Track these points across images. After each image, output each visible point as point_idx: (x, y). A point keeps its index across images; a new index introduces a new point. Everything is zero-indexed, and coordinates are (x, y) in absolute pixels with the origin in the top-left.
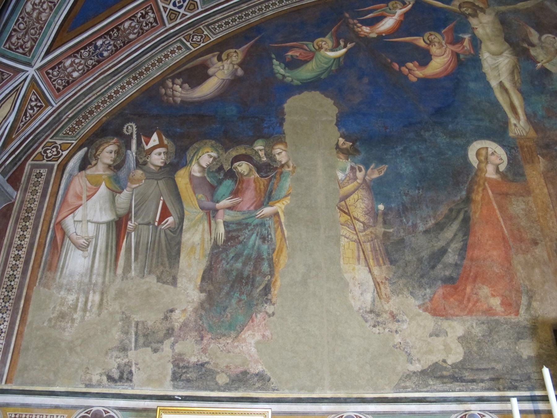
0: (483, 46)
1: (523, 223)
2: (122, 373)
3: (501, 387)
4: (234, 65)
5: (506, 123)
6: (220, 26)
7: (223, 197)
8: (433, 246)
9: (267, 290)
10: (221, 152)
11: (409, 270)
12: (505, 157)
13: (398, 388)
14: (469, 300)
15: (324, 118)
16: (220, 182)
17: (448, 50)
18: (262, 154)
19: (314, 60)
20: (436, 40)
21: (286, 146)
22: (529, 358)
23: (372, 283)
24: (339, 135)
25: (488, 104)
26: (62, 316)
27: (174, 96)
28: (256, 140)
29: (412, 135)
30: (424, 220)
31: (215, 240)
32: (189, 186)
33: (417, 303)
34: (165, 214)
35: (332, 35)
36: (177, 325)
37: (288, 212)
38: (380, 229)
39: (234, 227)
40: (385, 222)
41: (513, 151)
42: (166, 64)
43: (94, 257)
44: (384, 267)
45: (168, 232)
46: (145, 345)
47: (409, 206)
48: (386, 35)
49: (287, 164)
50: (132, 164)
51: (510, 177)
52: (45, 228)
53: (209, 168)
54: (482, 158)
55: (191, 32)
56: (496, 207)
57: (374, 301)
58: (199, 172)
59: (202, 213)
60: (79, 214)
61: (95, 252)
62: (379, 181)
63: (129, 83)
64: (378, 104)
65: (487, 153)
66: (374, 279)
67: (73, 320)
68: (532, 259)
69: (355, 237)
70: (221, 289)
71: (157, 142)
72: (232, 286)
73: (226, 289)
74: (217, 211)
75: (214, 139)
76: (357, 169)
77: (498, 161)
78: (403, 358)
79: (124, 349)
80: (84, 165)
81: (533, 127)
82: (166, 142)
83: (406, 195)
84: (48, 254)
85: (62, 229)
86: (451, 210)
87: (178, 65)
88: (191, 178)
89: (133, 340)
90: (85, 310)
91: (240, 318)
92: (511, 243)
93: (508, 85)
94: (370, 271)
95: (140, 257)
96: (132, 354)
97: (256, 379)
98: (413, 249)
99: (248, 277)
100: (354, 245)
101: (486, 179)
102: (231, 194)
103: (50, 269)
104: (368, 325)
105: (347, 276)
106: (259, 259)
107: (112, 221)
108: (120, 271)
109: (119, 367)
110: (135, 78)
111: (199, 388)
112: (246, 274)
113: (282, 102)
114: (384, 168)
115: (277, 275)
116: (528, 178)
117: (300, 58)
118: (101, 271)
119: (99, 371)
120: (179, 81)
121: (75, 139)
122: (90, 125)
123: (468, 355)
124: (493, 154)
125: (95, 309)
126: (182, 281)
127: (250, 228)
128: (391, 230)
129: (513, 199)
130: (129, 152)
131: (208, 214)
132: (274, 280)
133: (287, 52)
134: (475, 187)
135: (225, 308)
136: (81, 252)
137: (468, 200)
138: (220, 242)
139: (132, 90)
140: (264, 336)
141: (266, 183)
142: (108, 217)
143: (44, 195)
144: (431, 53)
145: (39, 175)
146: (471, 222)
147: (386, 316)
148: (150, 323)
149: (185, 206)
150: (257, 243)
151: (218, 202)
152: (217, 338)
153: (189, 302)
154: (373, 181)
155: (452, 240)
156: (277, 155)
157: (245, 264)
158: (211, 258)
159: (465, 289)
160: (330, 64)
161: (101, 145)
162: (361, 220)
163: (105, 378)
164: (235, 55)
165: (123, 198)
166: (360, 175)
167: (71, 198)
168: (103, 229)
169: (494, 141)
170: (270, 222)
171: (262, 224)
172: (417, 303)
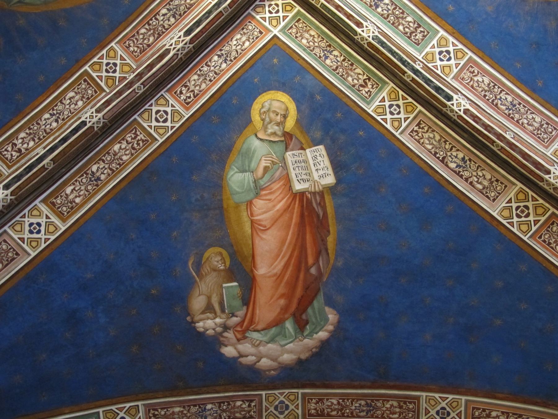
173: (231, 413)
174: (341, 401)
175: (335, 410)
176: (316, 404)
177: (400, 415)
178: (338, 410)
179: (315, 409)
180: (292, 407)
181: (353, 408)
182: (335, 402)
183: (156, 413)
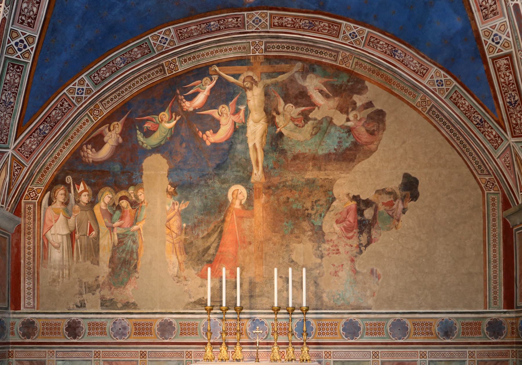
0: (250, 117)
1: (247, 233)
2: (81, 304)
4: (117, 134)
5: (251, 173)
6: (108, 102)
7: (116, 221)
8: (205, 245)
9: (136, 267)
10: (114, 194)
11: (193, 257)
12: (246, 196)
14: (216, 271)
15: (162, 173)
16: (114, 212)
17: (230, 119)
18: (132, 195)
19: (158, 130)
20: (225, 112)
21: (144, 190)
23: (177, 263)
24: (168, 183)
25: (244, 160)
26: (54, 281)
27: (88, 157)
28: (129, 187)
29: (203, 182)
30: (203, 232)
32: (100, 214)
33: (196, 272)
34: (91, 230)
35: (168, 111)
36: (101, 283)
37: (144, 228)
38: (183, 237)
39: (121, 236)
40: (185, 233)
41: (251, 191)
42: (81, 133)
43: (63, 252)
44: (183, 256)
45: (93, 239)
46: (89, 292)
47: (196, 224)
48: (198, 109)
49: (144, 201)
50: (73, 202)
51: (246, 206)
52: (39, 238)
53: (109, 204)
54: (235, 196)
55: (92, 107)
56: (236, 225)
57: (178, 271)
58: (105, 207)
59: (107, 229)
60: (53, 230)
61: (63, 250)
62: (186, 211)
63: (64, 148)
64: (188, 162)
66: (179, 261)
67: (59, 282)
68: (247, 252)
69: (172, 241)
70: (117, 267)
71: (83, 189)
72: (122, 265)
73: (119, 266)
74: (113, 228)
75: (110, 186)
77: (242, 198)
79: (81, 294)
80: (50, 202)
81: (265, 175)
82: (87, 188)
83: (196, 218)
84: (42, 252)
85: (46, 238)
86: (215, 226)
87: (88, 134)
88: (101, 209)
89: (84, 290)
90: (63, 277)
91: (126, 279)
92: (239, 243)
93: (258, 146)
94: (177, 258)
95: (83, 252)
96: (84, 296)
97: (132, 305)
98: (196, 247)
99: (128, 261)
100: (171, 245)
101: (234, 209)
102: (119, 219)
103: (45, 259)
104: (175, 282)
105: (168, 260)
106: (132, 252)
107: (68, 234)
108: (75, 259)
109: (80, 302)
110: (67, 144)
111: (111, 309)
112: (127, 259)
113: (142, 162)
114: (188, 203)
115: (139, 259)
116: (255, 207)
117: (151, 129)
118: (67, 259)
119: (72, 303)
120: (90, 146)
121: (42, 186)
122: (48, 177)
124: (240, 193)
125: (67, 277)
126: (101, 263)
127: (128, 237)
128: (188, 237)
129: (245, 219)
130: (70, 194)
131: (110, 230)
132: (138, 262)
133: (144, 125)
134: (228, 213)
135: (119, 275)
136: (56, 250)
137: (223, 221)
138: (116, 244)
139: (66, 153)
140: (135, 287)
141: (135, 212)
142: (66, 232)
143: (34, 220)
144: (221, 123)
145: (29, 208)
146: (223, 233)
147: (182, 278)
148: (90, 283)
149: (99, 226)
151: (114, 223)
152: (116, 288)
153: (105, 273)
154: (182, 210)
155: (213, 242)
157: (127, 254)
158: (113, 252)
159: (215, 266)
160: (166, 133)
161: (56, 190)
162: (175, 232)
163: (75, 306)
164: (117, 126)
165: (71, 221)
166: (176, 207)
167: (47, 222)
168: (65, 237)
169: (243, 185)
170: (136, 234)
171: (133, 235)
173: (226, 25)
174: (294, 19)
175: (290, 24)
176: (278, 20)
177: (328, 31)
178: (292, 24)
179: (278, 23)
180: (263, 21)
181: (301, 24)
182: (290, 19)
183: (181, 31)
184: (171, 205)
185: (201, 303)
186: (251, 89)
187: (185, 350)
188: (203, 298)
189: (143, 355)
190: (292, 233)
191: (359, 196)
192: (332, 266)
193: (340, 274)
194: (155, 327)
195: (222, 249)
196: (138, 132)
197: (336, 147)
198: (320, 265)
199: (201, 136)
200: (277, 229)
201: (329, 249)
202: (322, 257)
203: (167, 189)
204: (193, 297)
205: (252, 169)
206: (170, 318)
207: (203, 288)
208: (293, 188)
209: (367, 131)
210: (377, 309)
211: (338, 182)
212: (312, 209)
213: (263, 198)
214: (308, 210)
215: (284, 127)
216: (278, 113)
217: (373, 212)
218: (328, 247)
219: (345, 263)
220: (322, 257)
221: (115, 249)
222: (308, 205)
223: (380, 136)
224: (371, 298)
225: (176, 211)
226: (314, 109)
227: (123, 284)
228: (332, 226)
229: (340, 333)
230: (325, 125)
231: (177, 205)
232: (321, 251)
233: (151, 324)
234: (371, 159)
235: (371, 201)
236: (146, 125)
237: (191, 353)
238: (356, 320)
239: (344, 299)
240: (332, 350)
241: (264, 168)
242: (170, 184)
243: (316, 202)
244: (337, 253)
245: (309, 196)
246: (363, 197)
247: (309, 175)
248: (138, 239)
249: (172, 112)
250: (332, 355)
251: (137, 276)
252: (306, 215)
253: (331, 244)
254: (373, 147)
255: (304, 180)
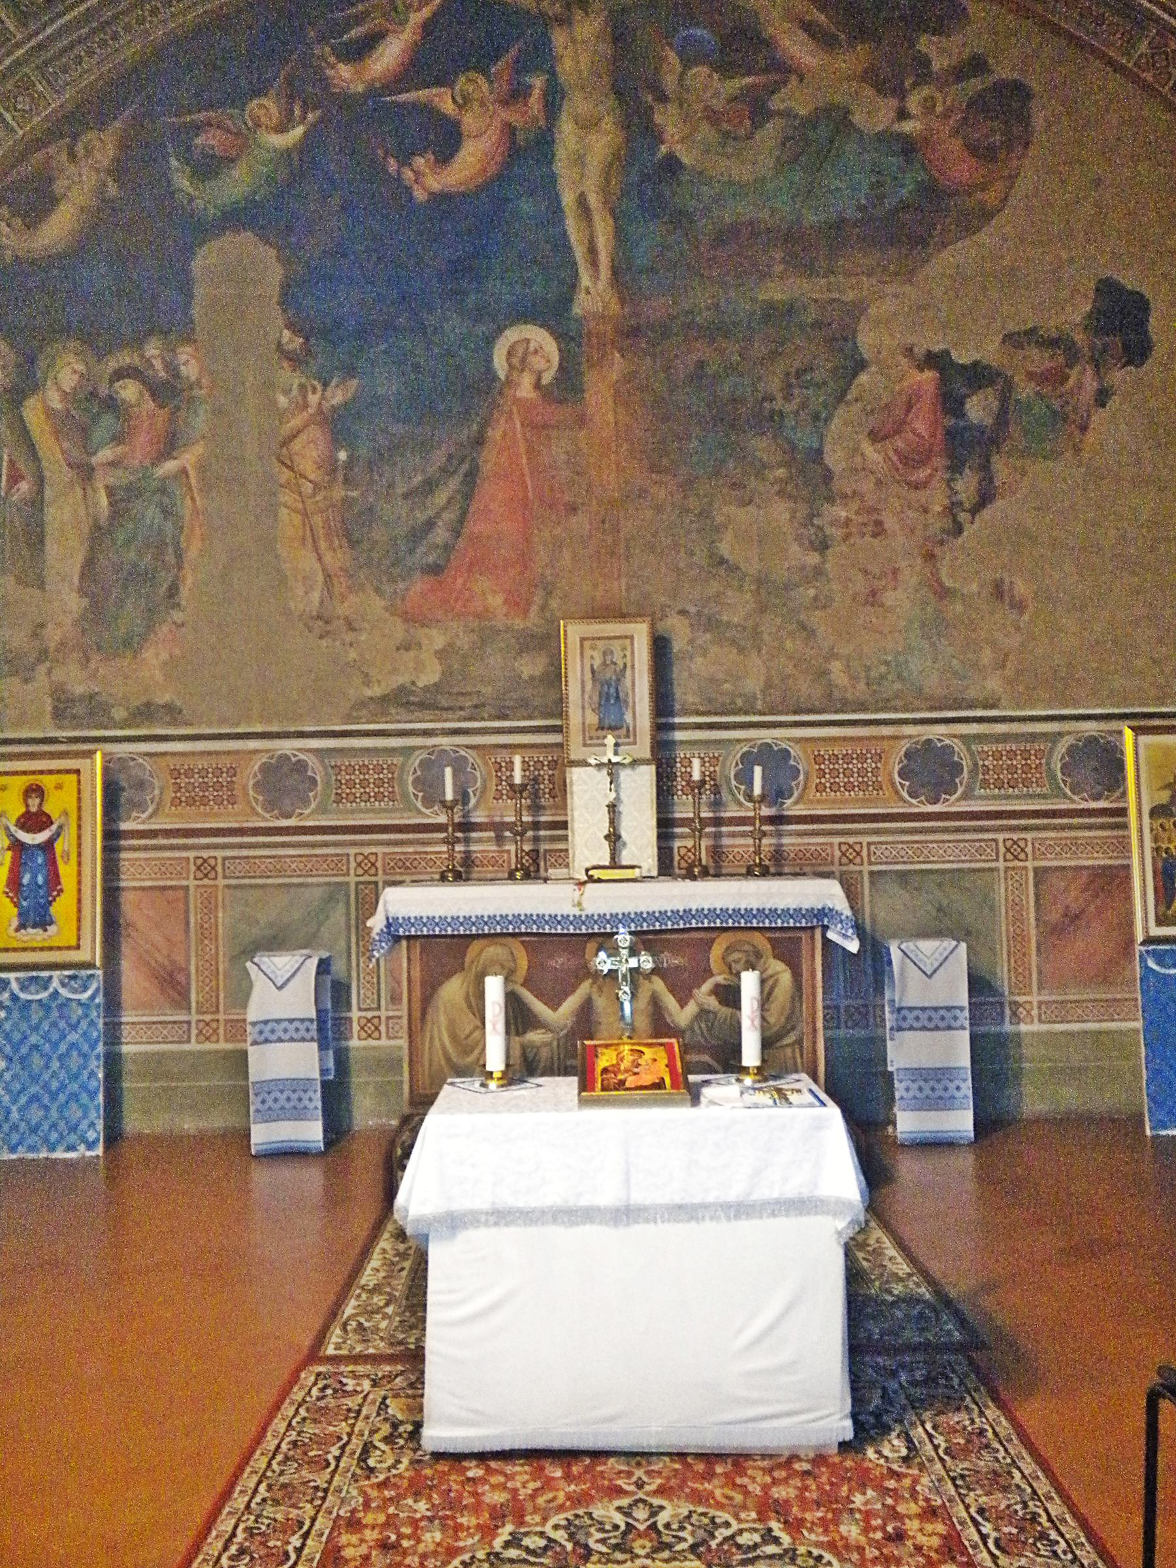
0: (565, 107)
3: (486, 716)
5: (573, 286)
7: (102, 445)
10: (92, 361)
13: (349, 719)
16: (95, 419)
18: (158, 364)
22: (532, 678)
23: (320, 578)
31: (96, 520)
33: (383, 603)
37: (202, 468)
40: (346, 480)
49: (198, 381)
54: (515, 361)
57: (322, 602)
59: (67, 474)
65: (528, 348)
69: (300, 506)
72: (125, 587)
76: (309, 388)
78: (358, 681)
86: (450, 457)
93: (593, 200)
94: (320, 559)
100: (297, 519)
101: (517, 401)
102: (113, 438)
105: (286, 567)
123: (447, 673)
124: (536, 352)
128: (355, 494)
137: (479, 441)
147: (339, 624)
150: (156, 521)
151: (94, 453)
154: (334, 409)
155: (444, 509)
156: (182, 368)
162: (312, 477)
171: (163, 491)
172: (383, 603)
184: (295, 392)
185: (404, 700)
186: (564, 21)
187: (352, 851)
188: (413, 683)
189: (205, 868)
190: (717, 473)
191: (946, 353)
192: (860, 576)
193: (889, 598)
194: (250, 774)
195: (474, 527)
196: (174, 163)
197: (863, 202)
198: (818, 572)
199: (394, 174)
200: (665, 462)
201: (848, 520)
202: (823, 546)
203: (279, 344)
204: (379, 682)
205: (576, 275)
206: (299, 750)
207: (412, 654)
208: (716, 331)
209: (973, 149)
210: (1018, 707)
211: (872, 311)
212: (788, 397)
213: (617, 365)
214: (772, 399)
215: (682, 140)
216: (663, 98)
217: (996, 405)
218: (844, 514)
219: (903, 564)
220: (823, 546)
221: (98, 535)
222: (774, 384)
223: (1015, 163)
224: (999, 672)
225: (311, 411)
226: (785, 83)
227: (131, 644)
228: (856, 449)
229: (893, 784)
230: (823, 131)
231: (314, 392)
232: (820, 528)
233: (233, 772)
234: (986, 237)
235: (988, 367)
236: (198, 141)
237: (372, 858)
238: (947, 742)
239: (900, 677)
240: (866, 839)
241: (615, 271)
242: (290, 326)
243: (799, 374)
244: (875, 535)
245: (774, 355)
246: (962, 357)
247: (775, 292)
248: (179, 503)
249: (291, 97)
250: (864, 853)
251: (179, 622)
252: (766, 413)
253: (854, 505)
254: (990, 197)
255: (757, 307)
